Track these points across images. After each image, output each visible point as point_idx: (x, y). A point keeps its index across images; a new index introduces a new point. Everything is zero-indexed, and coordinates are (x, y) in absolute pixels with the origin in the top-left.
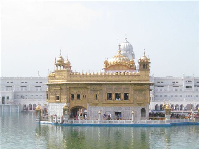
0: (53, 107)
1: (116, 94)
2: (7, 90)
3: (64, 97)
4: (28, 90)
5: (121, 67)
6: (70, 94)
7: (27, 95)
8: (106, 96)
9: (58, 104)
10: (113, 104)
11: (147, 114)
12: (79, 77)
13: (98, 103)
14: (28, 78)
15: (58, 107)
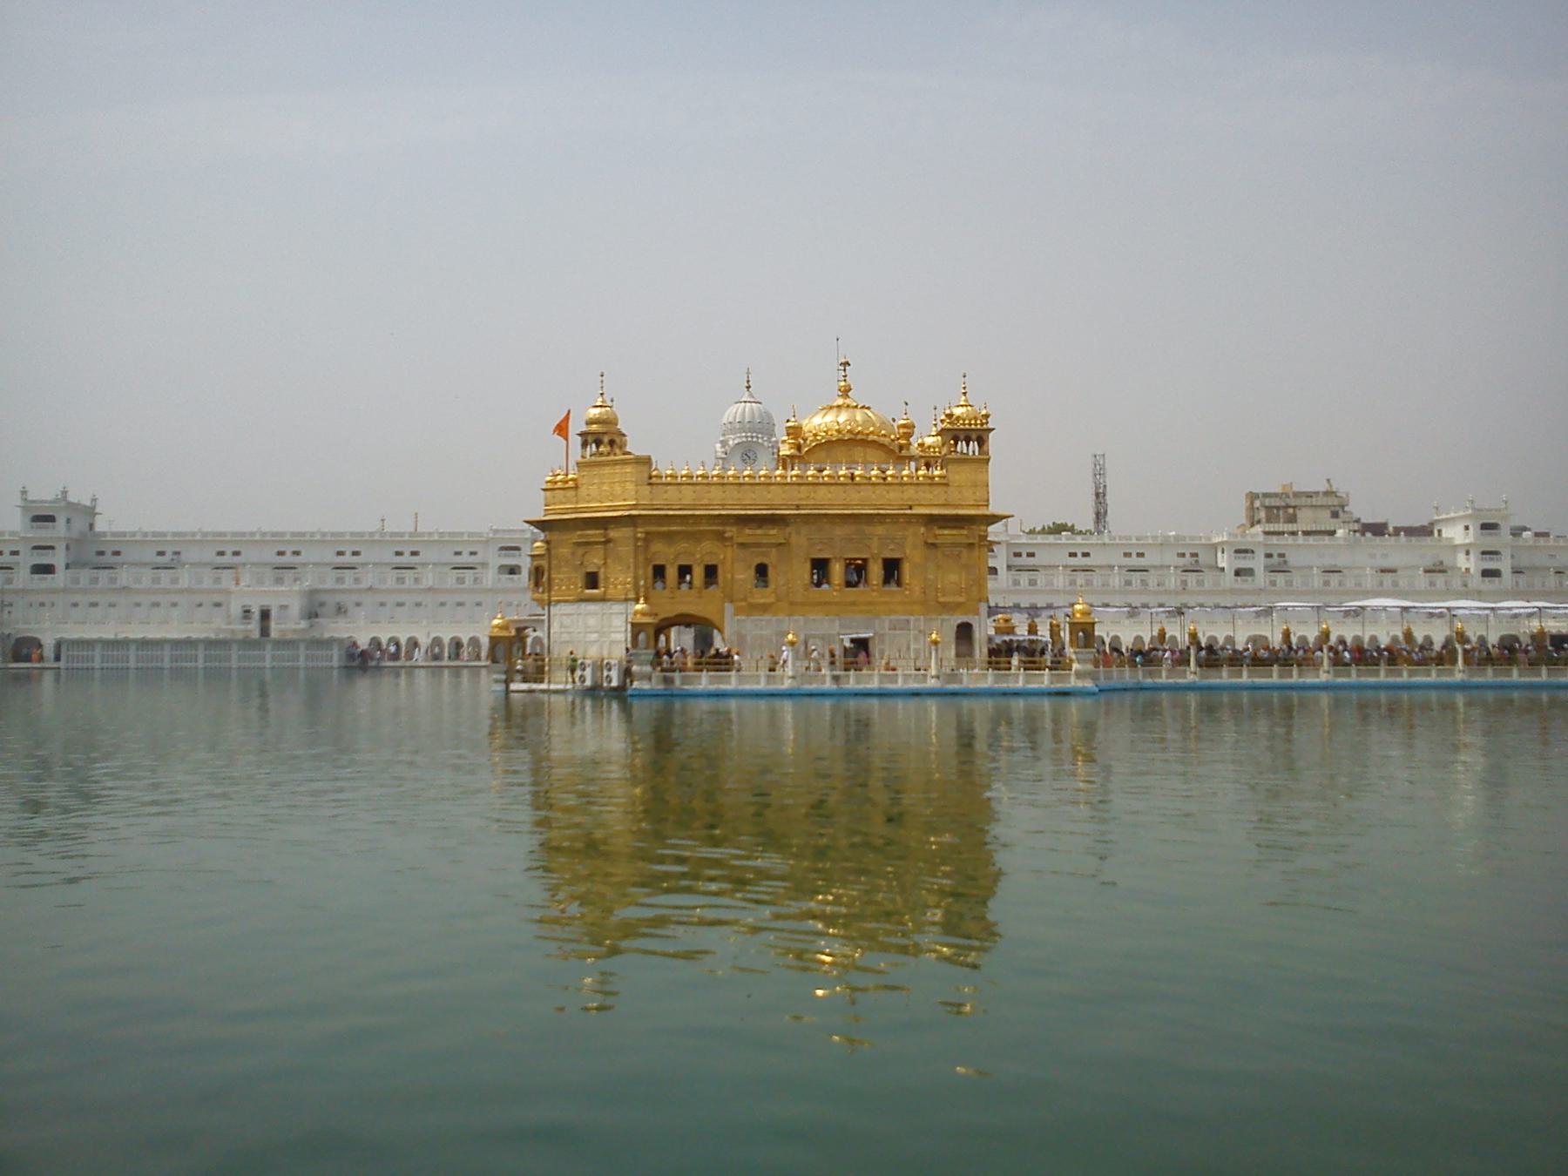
0: (567, 621)
1: (849, 563)
2: (279, 581)
3: (619, 577)
4: (364, 585)
5: (859, 452)
6: (647, 561)
7: (358, 604)
8: (804, 572)
9: (592, 607)
10: (836, 604)
11: (980, 651)
12: (688, 490)
13: (772, 600)
14: (362, 534)
15: (592, 621)
